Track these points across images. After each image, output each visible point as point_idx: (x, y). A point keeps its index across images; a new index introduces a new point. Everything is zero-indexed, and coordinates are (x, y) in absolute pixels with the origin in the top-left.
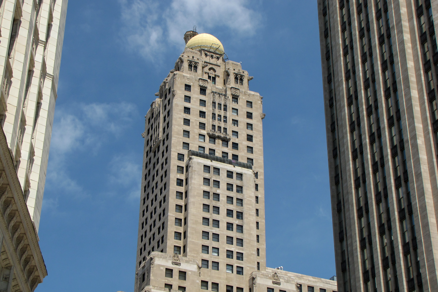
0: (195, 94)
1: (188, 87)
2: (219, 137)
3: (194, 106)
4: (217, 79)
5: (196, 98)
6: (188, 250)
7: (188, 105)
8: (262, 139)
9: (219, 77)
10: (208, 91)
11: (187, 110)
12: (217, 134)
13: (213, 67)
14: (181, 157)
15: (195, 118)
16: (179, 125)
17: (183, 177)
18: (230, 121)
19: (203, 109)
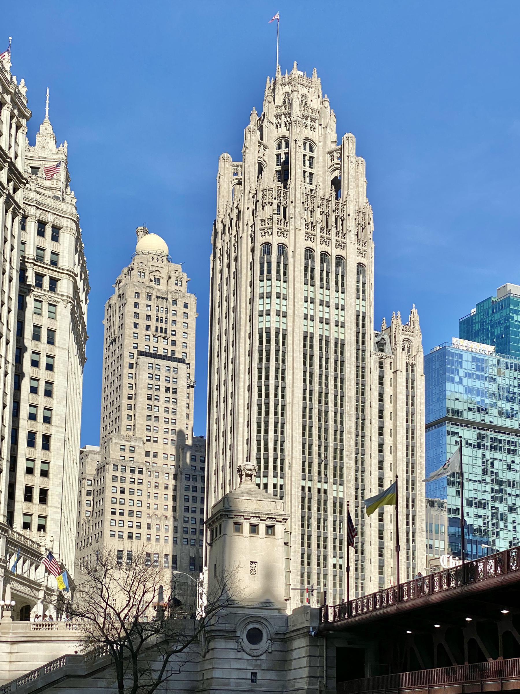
0: (143, 301)
1: (137, 294)
2: (161, 336)
3: (143, 311)
4: (161, 280)
5: (144, 304)
6: (137, 417)
7: (137, 310)
8: (195, 335)
9: (163, 278)
10: (153, 297)
11: (136, 315)
12: (159, 334)
13: (158, 269)
14: (132, 355)
15: (142, 322)
16: (130, 329)
17: (133, 381)
18: (170, 322)
19: (149, 314)
